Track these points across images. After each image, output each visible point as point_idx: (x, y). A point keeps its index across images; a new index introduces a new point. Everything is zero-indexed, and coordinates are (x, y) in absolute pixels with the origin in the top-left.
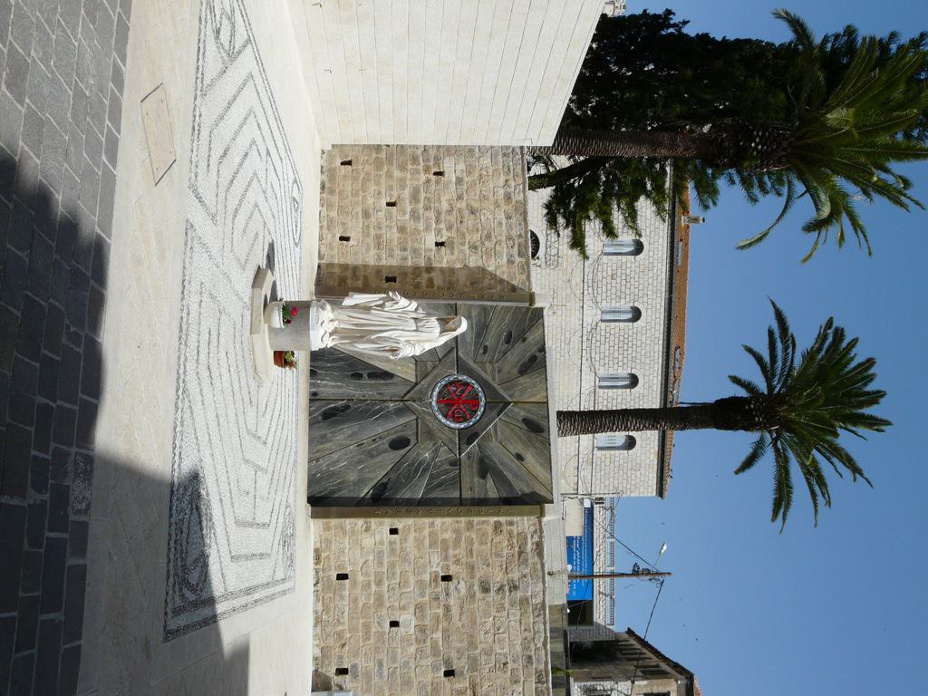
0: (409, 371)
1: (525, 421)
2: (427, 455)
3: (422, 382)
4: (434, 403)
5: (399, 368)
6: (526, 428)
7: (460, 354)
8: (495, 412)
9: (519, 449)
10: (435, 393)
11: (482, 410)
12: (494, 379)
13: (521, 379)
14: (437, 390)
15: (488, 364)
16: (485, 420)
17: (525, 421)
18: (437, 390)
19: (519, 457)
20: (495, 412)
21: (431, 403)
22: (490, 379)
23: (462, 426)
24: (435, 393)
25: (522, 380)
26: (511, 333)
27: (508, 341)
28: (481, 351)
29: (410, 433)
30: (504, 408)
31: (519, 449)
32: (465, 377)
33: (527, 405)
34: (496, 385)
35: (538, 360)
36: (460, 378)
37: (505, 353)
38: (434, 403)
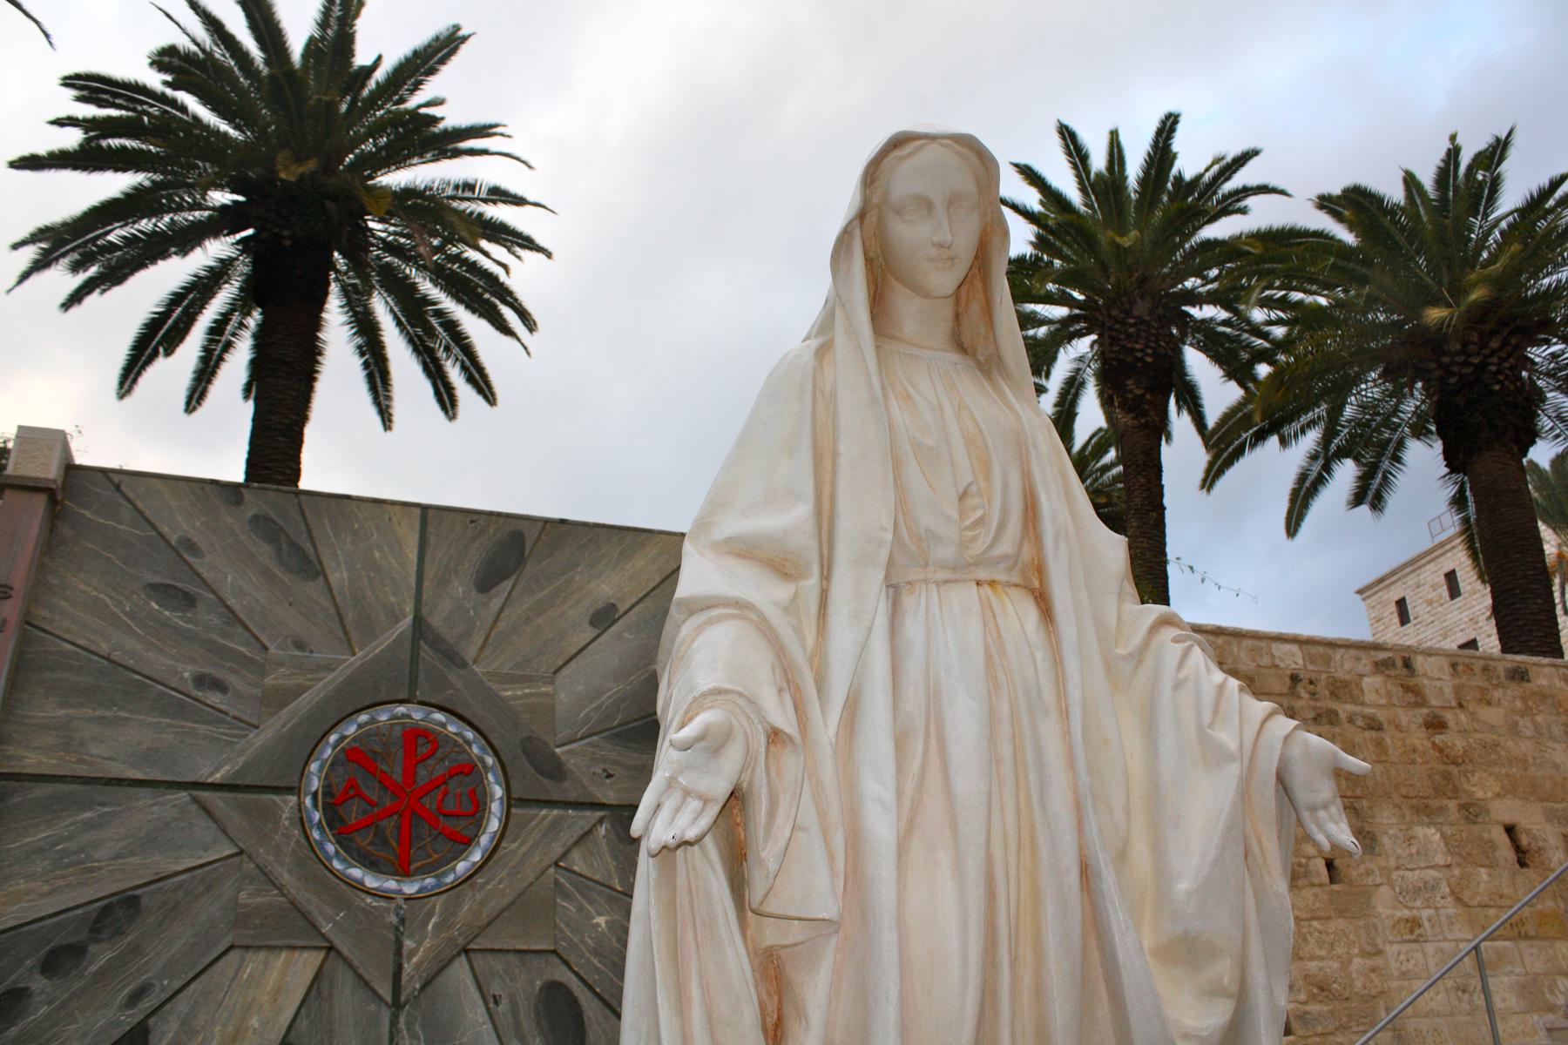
0: (273, 978)
1: (485, 584)
2: (601, 920)
3: (326, 928)
4: (410, 888)
5: (254, 1022)
6: (507, 585)
7: (218, 777)
8: (454, 677)
9: (577, 611)
10: (371, 882)
11: (439, 716)
12: (329, 668)
13: (334, 577)
14: (356, 873)
15: (269, 681)
16: (475, 711)
17: (485, 584)
18: (356, 873)
19: (605, 617)
20: (454, 677)
21: (408, 899)
22: (330, 680)
23: (498, 791)
24: (371, 882)
25: (338, 576)
26: (154, 587)
27: (189, 601)
28: (214, 698)
29: (525, 984)
30: (437, 642)
31: (577, 611)
32: (314, 767)
33: (430, 571)
34: (355, 661)
35: (271, 513)
36: (315, 784)
37: (232, 617)
38: (410, 888)
